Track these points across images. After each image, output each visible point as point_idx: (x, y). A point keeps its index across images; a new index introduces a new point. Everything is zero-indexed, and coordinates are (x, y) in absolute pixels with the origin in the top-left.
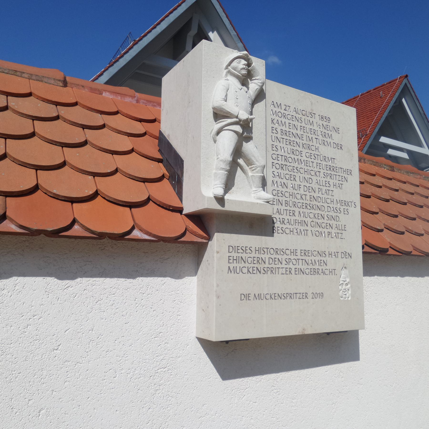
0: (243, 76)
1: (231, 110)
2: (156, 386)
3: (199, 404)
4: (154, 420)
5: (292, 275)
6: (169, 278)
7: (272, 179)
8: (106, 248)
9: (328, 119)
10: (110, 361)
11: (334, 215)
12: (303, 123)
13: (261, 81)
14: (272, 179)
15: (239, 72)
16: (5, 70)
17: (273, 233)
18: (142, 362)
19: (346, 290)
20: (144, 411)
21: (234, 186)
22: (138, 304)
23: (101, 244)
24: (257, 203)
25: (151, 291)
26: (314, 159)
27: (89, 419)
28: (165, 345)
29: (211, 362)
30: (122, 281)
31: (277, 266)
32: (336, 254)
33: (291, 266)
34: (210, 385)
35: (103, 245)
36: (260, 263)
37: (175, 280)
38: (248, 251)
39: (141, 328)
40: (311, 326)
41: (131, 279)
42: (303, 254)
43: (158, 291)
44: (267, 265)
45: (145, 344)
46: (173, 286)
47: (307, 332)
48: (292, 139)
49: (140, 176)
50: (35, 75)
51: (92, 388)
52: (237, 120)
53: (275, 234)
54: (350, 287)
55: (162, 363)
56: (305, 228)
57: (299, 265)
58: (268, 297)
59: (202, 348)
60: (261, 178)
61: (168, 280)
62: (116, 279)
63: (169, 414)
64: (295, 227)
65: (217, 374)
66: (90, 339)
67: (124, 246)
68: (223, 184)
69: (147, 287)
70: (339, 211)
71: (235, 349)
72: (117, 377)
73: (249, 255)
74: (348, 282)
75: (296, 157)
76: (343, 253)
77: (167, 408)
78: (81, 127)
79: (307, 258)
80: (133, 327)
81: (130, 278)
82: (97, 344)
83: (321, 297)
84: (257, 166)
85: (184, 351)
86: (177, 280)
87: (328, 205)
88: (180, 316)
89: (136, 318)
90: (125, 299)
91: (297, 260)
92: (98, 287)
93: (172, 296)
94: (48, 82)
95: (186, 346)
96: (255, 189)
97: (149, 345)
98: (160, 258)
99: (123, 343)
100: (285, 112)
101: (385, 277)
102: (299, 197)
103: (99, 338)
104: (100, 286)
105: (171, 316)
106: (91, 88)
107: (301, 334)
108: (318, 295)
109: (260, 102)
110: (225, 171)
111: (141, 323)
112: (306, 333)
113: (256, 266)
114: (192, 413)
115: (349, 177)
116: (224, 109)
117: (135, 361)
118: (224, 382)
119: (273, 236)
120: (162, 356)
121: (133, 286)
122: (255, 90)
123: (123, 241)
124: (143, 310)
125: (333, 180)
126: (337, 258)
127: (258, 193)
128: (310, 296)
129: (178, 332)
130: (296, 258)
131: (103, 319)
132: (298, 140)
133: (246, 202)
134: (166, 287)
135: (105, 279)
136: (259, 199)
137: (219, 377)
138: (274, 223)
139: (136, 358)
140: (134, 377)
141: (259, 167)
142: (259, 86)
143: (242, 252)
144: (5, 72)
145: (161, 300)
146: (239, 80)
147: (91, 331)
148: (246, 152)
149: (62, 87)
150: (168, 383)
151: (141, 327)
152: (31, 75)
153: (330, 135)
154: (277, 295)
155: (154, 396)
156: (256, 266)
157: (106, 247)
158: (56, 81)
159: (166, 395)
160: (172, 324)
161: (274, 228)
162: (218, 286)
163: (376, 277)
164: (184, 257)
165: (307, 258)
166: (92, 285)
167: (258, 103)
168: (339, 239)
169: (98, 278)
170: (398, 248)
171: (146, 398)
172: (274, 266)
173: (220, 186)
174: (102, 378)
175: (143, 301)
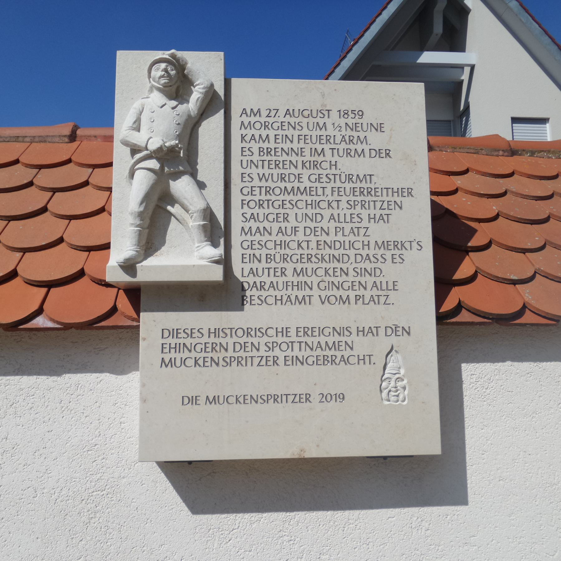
0: (164, 87)
1: (137, 141)
2: (90, 512)
3: (155, 543)
4: (89, 556)
5: (278, 367)
6: (108, 374)
7: (242, 224)
8: (23, 340)
9: (361, 114)
10: (28, 477)
11: (368, 266)
12: (305, 128)
13: (202, 86)
14: (242, 224)
15: (158, 83)
16: (6, 138)
17: (243, 304)
18: (70, 481)
19: (398, 388)
20: (74, 542)
21: (164, 246)
22: (64, 408)
23: (16, 336)
24: (194, 265)
25: (82, 392)
26: (326, 182)
27: (3, 543)
28: (103, 461)
29: (173, 488)
30: (42, 380)
31: (251, 354)
32: (372, 331)
33: (277, 352)
34: (172, 518)
35: (19, 336)
36: (216, 351)
37: (117, 376)
38: (196, 334)
39: (69, 438)
40: (318, 446)
41: (54, 377)
42: (301, 334)
43: (93, 391)
44: (230, 353)
45: (74, 458)
46: (114, 384)
47: (307, 455)
48: (281, 159)
49: (82, 245)
50: (38, 136)
51: (7, 507)
52: (148, 152)
53: (247, 307)
54: (406, 383)
55: (98, 484)
56: (308, 292)
57: (292, 350)
58: (232, 400)
59: (158, 467)
60: (201, 228)
61: (106, 377)
62: (35, 377)
63: (110, 551)
64: (286, 292)
65: (183, 505)
66: (3, 449)
67: (45, 336)
68: (135, 245)
69: (77, 385)
70: (381, 260)
71: (213, 472)
72: (37, 497)
73: (197, 340)
74: (403, 376)
75: (289, 186)
76: (391, 327)
77: (107, 542)
78: (51, 191)
79: (309, 340)
80: (58, 437)
81: (54, 375)
82: (13, 456)
83: (338, 400)
84: (193, 212)
85: (130, 470)
86: (119, 377)
87: (357, 252)
88: (124, 423)
89: (62, 425)
90: (47, 402)
91: (290, 344)
92: (12, 387)
93: (112, 397)
94: (53, 141)
95: (133, 464)
96: (197, 245)
97: (80, 460)
98: (95, 349)
99: (44, 456)
100: (268, 119)
101: (532, 363)
102: (294, 245)
103: (15, 449)
104: (15, 386)
105: (111, 424)
106: (105, 136)
107: (296, 456)
108: (334, 397)
109: (213, 115)
110: (136, 227)
111: (69, 431)
112: (306, 457)
113: (210, 355)
114: (144, 553)
115: (406, 201)
116: (129, 142)
117: (61, 479)
118: (195, 516)
119: (242, 310)
120: (99, 475)
121: (58, 385)
122: (195, 101)
123: (18, 332)
124: (71, 416)
125: (368, 211)
126: (376, 337)
127: (201, 251)
128: (315, 398)
129: (122, 444)
130: (287, 340)
131: (19, 425)
132: (294, 158)
133: (173, 266)
134: (104, 386)
135: (21, 377)
136: (202, 258)
137: (186, 508)
138: (243, 289)
139: (63, 475)
140: (60, 499)
141: (195, 213)
142: (201, 93)
143: (186, 336)
144: (6, 141)
145: (97, 402)
146: (163, 94)
147: (5, 440)
148: (176, 194)
149: (68, 143)
150: (107, 511)
151: (69, 437)
152: (34, 137)
153: (362, 138)
154: (249, 397)
155: (87, 526)
156: (210, 355)
157: (22, 338)
158: (62, 138)
159: (105, 525)
160: (112, 435)
161: (245, 298)
162: (144, 386)
163: (509, 363)
164: (129, 345)
165: (309, 340)
166: (6, 385)
167: (210, 118)
168: (380, 306)
169: (12, 377)
170: (545, 312)
171: (76, 527)
172: (244, 355)
173: (129, 248)
174: (19, 497)
175: (71, 403)
